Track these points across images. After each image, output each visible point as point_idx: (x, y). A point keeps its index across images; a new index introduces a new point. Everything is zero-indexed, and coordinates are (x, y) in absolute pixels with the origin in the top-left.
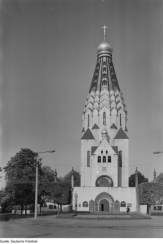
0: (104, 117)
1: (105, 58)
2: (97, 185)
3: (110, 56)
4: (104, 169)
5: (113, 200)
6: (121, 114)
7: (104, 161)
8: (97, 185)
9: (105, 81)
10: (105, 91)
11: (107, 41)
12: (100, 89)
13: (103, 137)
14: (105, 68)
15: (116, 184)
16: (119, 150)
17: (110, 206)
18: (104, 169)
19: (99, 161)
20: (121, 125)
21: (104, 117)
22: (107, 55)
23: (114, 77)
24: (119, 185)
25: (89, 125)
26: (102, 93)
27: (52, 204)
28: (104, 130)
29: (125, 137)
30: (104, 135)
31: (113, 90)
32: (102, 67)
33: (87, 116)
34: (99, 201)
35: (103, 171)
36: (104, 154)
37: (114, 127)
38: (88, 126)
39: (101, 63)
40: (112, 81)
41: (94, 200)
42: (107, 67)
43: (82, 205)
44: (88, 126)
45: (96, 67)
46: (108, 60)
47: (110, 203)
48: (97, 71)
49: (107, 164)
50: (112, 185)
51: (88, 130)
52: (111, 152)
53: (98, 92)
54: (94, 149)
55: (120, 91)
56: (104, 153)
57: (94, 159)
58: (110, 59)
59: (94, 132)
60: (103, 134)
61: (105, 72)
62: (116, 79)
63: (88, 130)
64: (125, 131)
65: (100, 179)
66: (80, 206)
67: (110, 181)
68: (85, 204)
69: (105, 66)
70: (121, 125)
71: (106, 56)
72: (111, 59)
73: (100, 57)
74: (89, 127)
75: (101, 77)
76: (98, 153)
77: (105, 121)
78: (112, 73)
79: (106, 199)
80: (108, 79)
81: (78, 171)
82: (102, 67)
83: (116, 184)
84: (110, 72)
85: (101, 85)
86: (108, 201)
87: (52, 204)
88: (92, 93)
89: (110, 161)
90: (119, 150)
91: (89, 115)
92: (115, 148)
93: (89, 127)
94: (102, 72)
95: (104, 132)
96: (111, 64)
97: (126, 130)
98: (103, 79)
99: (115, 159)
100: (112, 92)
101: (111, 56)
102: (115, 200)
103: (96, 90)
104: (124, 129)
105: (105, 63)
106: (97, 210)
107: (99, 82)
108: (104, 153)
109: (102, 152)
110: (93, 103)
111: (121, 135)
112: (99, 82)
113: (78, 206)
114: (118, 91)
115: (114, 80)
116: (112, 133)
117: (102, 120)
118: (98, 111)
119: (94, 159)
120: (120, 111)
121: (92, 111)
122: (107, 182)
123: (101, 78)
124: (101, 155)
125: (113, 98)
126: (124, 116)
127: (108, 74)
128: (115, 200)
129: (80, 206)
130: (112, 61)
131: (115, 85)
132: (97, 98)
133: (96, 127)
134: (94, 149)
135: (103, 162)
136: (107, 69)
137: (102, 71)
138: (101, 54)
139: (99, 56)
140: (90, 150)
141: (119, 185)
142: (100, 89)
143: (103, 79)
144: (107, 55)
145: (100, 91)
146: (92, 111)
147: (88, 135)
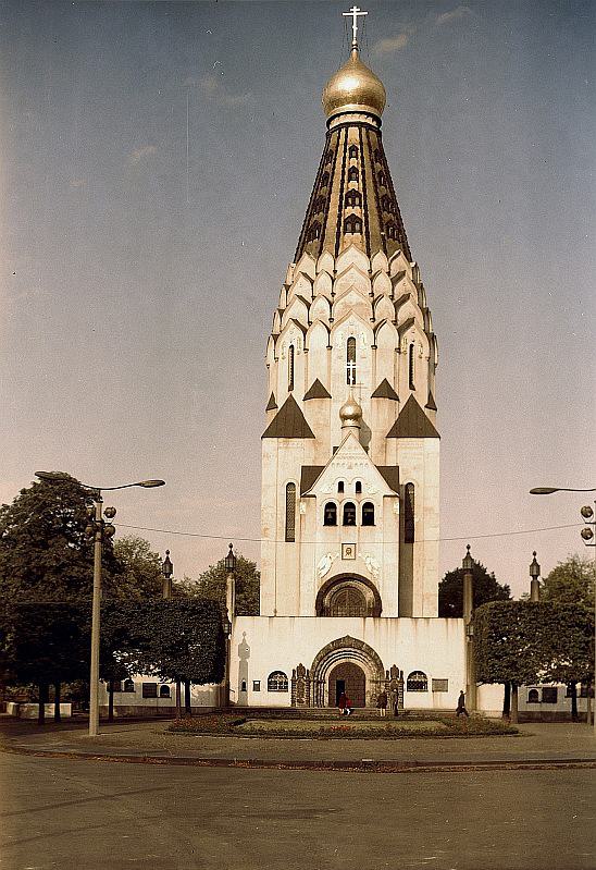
0: (351, 355)
1: (354, 131)
2: (322, 611)
3: (374, 124)
4: (348, 550)
5: (380, 666)
6: (412, 346)
7: (349, 520)
8: (322, 611)
9: (353, 219)
10: (353, 256)
11: (364, 68)
12: (337, 249)
13: (346, 431)
14: (354, 170)
15: (390, 606)
16: (403, 481)
17: (369, 686)
18: (348, 550)
19: (330, 520)
20: (412, 387)
21: (351, 355)
22: (363, 119)
23: (388, 203)
24: (404, 610)
25: (292, 384)
27: (156, 680)
28: (352, 402)
29: (428, 431)
30: (350, 422)
31: (385, 252)
32: (344, 166)
33: (287, 350)
34: (329, 671)
36: (350, 494)
37: (385, 391)
38: (291, 388)
39: (341, 149)
41: (308, 667)
42: (363, 166)
43: (264, 685)
44: (291, 388)
45: (323, 164)
46: (368, 137)
47: (368, 677)
48: (324, 179)
49: (357, 532)
50: (376, 611)
51: (291, 401)
52: (376, 489)
53: (327, 258)
54: (311, 474)
55: (410, 260)
56: (350, 489)
57: (311, 514)
58: (373, 135)
59: (310, 412)
60: (344, 418)
61: (353, 185)
62: (397, 213)
63: (291, 401)
64: (426, 411)
65: (334, 589)
66: (257, 688)
67: (369, 595)
68: (276, 682)
69: (354, 162)
70: (412, 387)
71: (359, 125)
72: (379, 134)
73: (339, 128)
74: (293, 393)
75: (341, 202)
76: (324, 489)
78: (383, 190)
79: (352, 661)
80: (366, 210)
81: (250, 559)
82: (344, 166)
83: (390, 606)
84: (372, 184)
86: (360, 669)
87: (156, 680)
88: (307, 263)
89: (369, 520)
90: (403, 481)
91: (292, 347)
92: (390, 474)
93: (293, 393)
94: (342, 185)
95: (350, 411)
96: (379, 155)
97: (431, 405)
98: (349, 211)
99: (388, 514)
100: (380, 260)
101: (379, 123)
102: (387, 667)
103: (320, 253)
104: (422, 401)
105: (354, 148)
106: (319, 700)
107: (332, 221)
108: (350, 489)
109: (341, 485)
110: (310, 300)
111: (413, 424)
112: (332, 221)
113: (250, 686)
114: (401, 259)
115: (387, 216)
116: (381, 416)
117: (341, 366)
118: (329, 332)
119: (311, 514)
120: (408, 334)
121: (305, 331)
122: (357, 597)
123: (340, 206)
124: (335, 497)
125: (383, 283)
126: (426, 353)
127: (364, 190)
128: (387, 667)
129: (257, 688)
130: (380, 145)
131: (391, 234)
132: (323, 282)
133: (318, 392)
134: (311, 474)
135: (346, 523)
136: (363, 172)
137: (343, 180)
138: (342, 114)
139: (335, 123)
140: (297, 479)
141: (404, 610)
142: (337, 249)
143: (349, 211)
144: (363, 119)
145: (337, 256)
146: (305, 331)
147: (289, 424)
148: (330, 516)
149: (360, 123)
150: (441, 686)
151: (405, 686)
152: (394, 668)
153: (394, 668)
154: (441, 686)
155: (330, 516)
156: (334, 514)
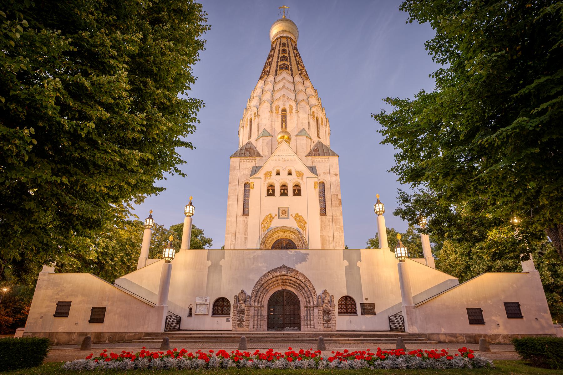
7: (284, 192)
19: (271, 192)
26: (279, 78)
35: (279, 218)
40: (298, 67)
41: (249, 293)
49: (289, 201)
56: (284, 174)
71: (287, 37)
77: (286, 116)
85: (277, 70)
89: (297, 191)
108: (284, 174)
111: (319, 150)
145: (276, 75)
147: (249, 151)
148: (271, 191)
149: (288, 37)
150: (369, 309)
151: (336, 308)
152: (325, 293)
153: (325, 293)
154: (369, 309)
155: (271, 191)
156: (273, 191)
